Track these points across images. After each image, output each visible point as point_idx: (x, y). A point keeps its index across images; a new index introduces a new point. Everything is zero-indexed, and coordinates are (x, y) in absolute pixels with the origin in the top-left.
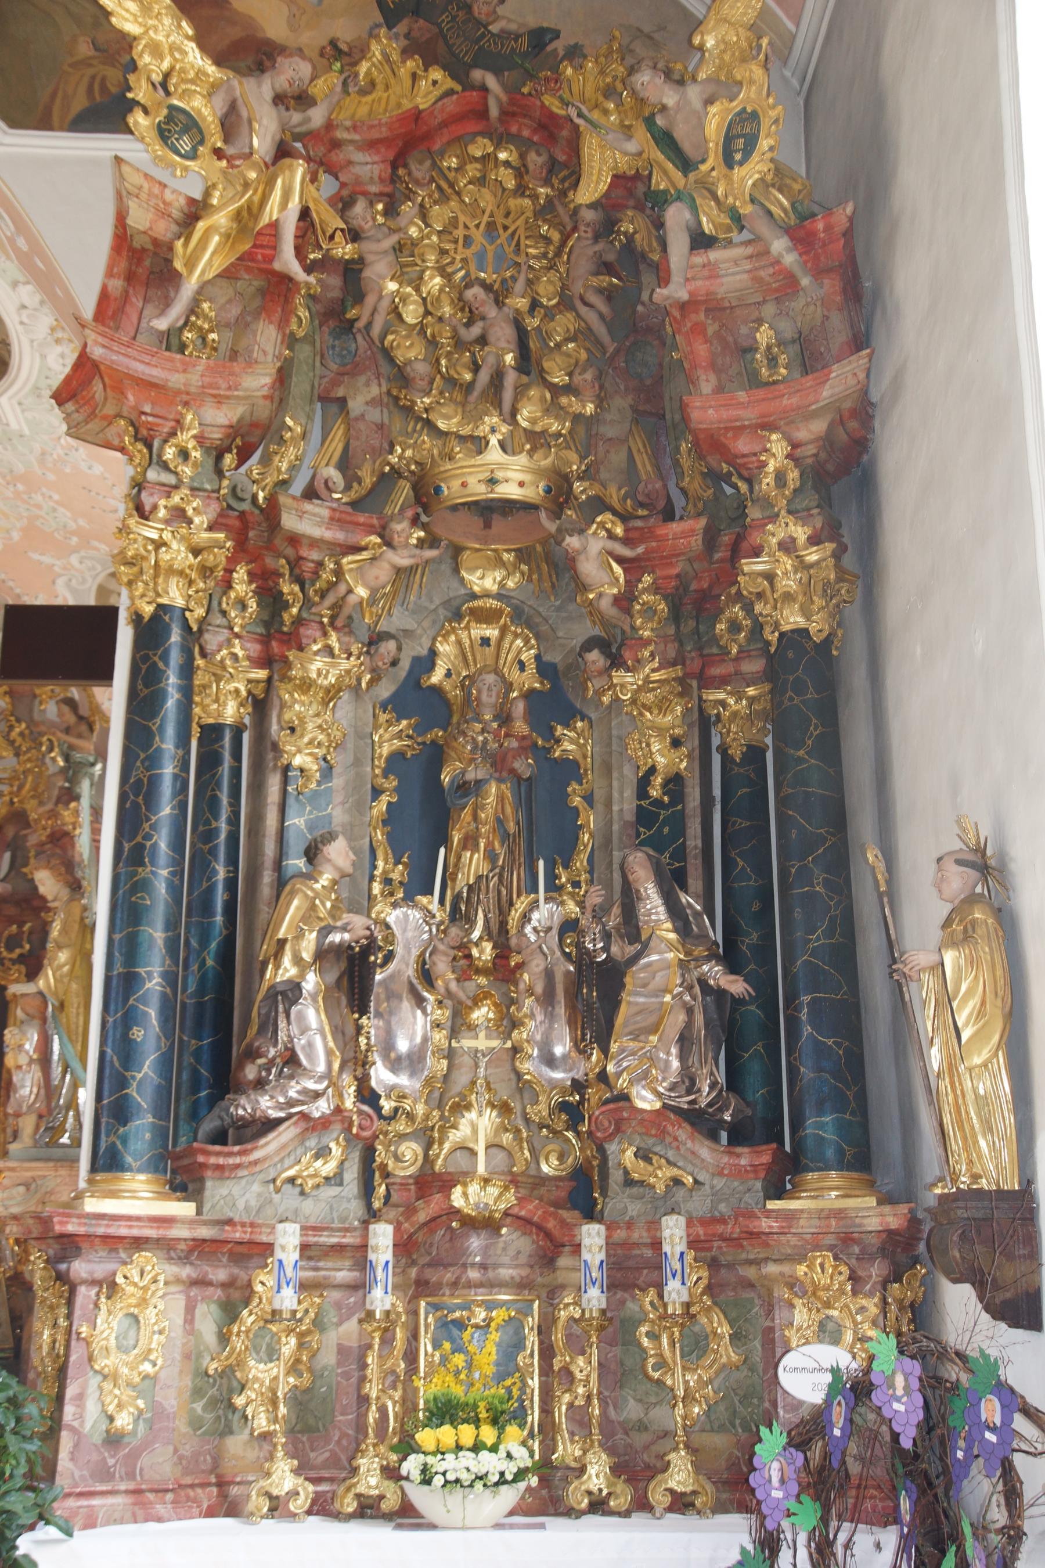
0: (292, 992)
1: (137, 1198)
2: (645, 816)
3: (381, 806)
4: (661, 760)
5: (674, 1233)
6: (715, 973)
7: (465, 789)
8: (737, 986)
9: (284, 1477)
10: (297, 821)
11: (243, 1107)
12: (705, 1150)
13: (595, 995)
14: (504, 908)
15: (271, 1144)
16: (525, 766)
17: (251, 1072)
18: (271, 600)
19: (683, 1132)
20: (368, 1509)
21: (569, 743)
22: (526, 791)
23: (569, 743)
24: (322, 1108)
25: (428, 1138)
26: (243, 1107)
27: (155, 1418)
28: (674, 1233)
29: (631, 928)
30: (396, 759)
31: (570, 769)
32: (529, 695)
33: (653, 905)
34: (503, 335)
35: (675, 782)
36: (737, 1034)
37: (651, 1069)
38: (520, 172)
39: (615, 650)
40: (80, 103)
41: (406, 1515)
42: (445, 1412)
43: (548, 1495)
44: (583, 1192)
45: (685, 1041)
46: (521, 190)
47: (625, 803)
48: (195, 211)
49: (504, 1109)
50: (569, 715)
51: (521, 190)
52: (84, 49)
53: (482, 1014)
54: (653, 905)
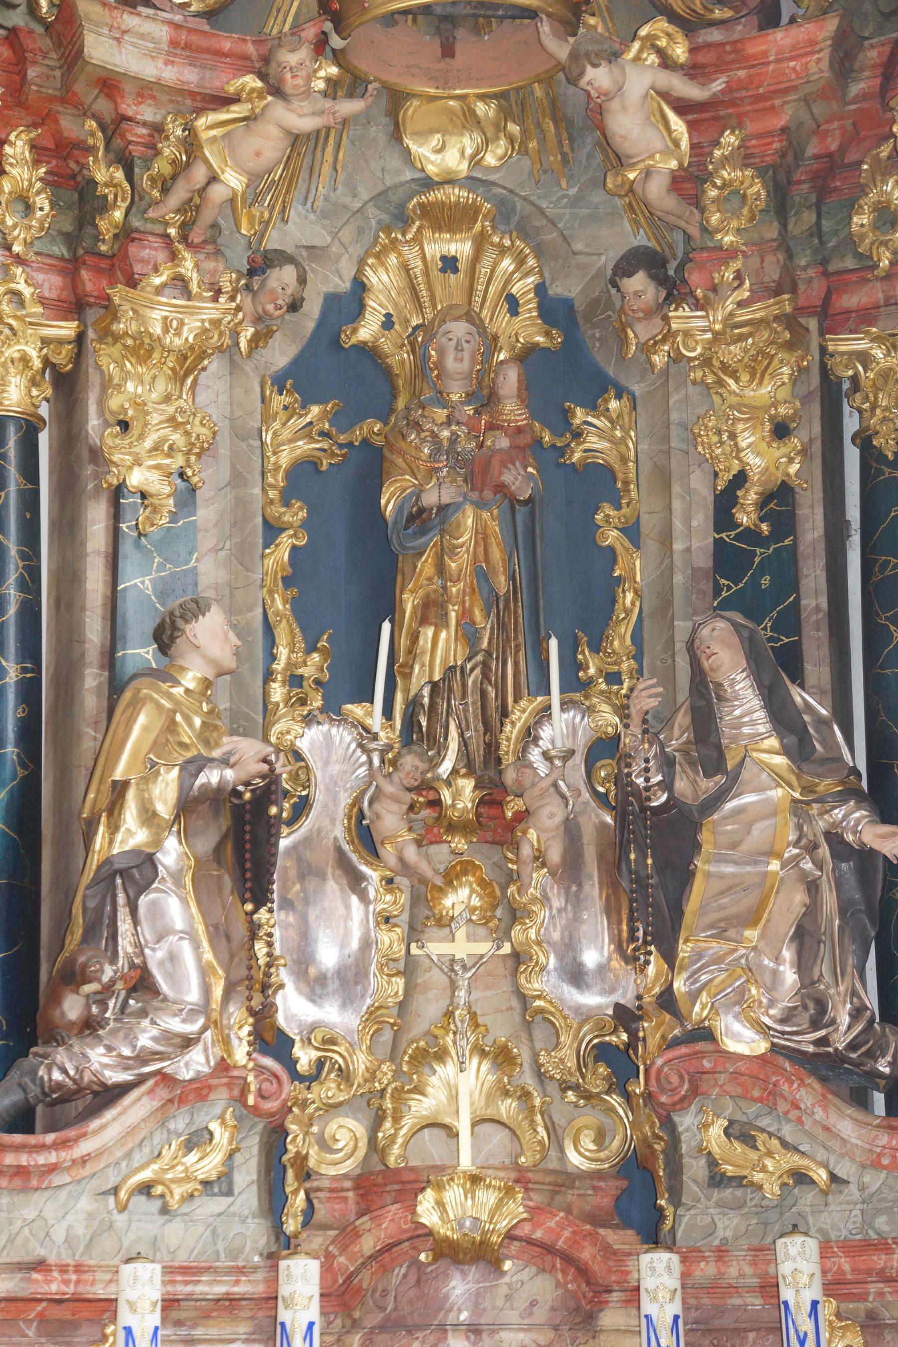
0: (140, 871)
2: (729, 559)
3: (281, 552)
4: (755, 462)
5: (799, 1266)
6: (858, 824)
10: (140, 581)
12: (846, 1124)
13: (650, 862)
14: (493, 719)
15: (110, 1128)
16: (521, 479)
17: (72, 1007)
18: (79, 199)
19: (807, 1093)
21: (599, 436)
22: (525, 521)
23: (599, 436)
24: (194, 1063)
26: (59, 1066)
28: (799, 1266)
29: (709, 747)
30: (303, 473)
31: (599, 483)
32: (527, 356)
33: (745, 709)
35: (780, 499)
37: (748, 991)
39: (671, 272)
44: (641, 1197)
45: (805, 936)
47: (695, 537)
49: (503, 1058)
50: (596, 388)
53: (460, 899)
54: (745, 709)
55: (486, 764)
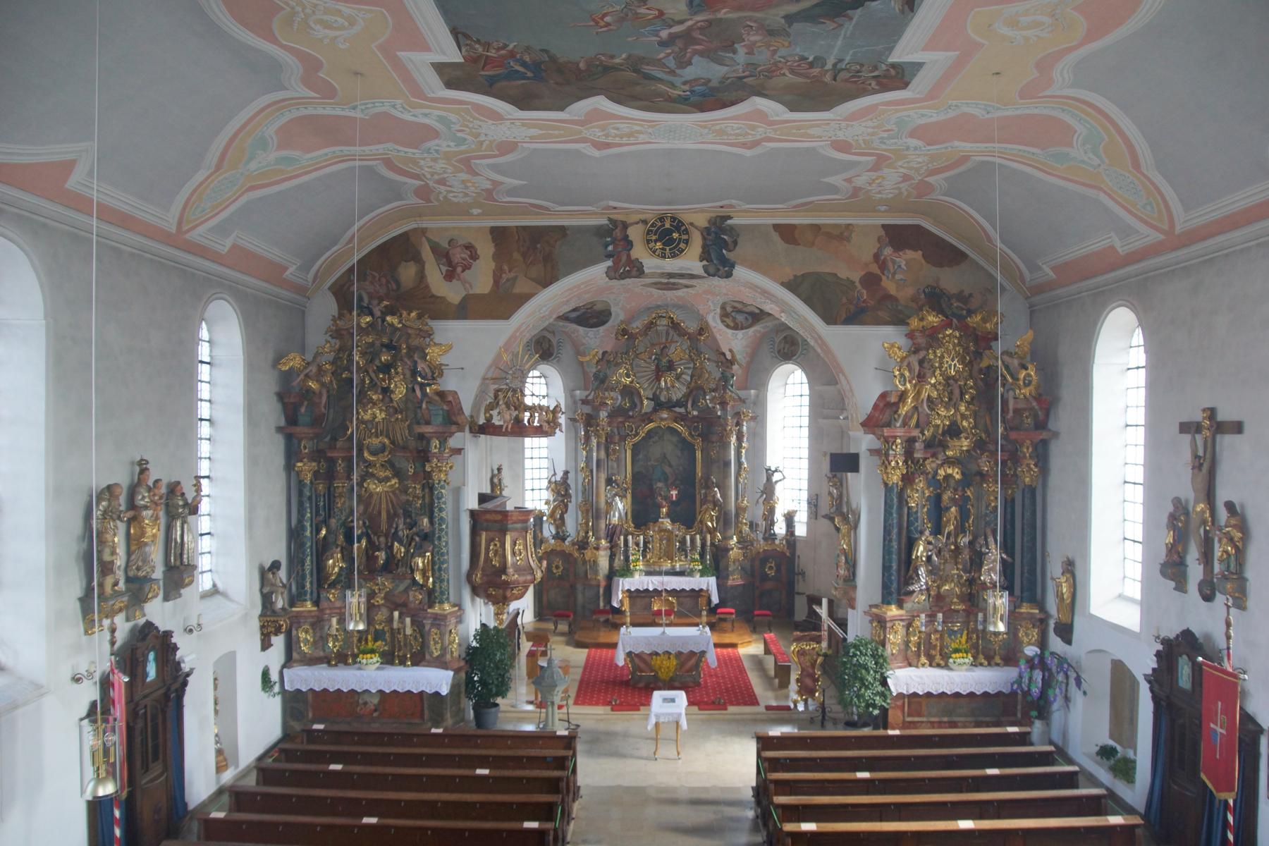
1: (893, 611)
6: (1004, 556)
7: (948, 509)
8: (1010, 560)
9: (923, 660)
11: (911, 588)
20: (939, 666)
25: (939, 587)
26: (911, 588)
27: (899, 651)
30: (928, 499)
34: (957, 392)
36: (1007, 569)
38: (959, 339)
40: (844, 316)
41: (946, 667)
42: (956, 651)
43: (975, 664)
46: (959, 344)
48: (903, 396)
51: (959, 344)
52: (844, 300)
55: (956, 544)
